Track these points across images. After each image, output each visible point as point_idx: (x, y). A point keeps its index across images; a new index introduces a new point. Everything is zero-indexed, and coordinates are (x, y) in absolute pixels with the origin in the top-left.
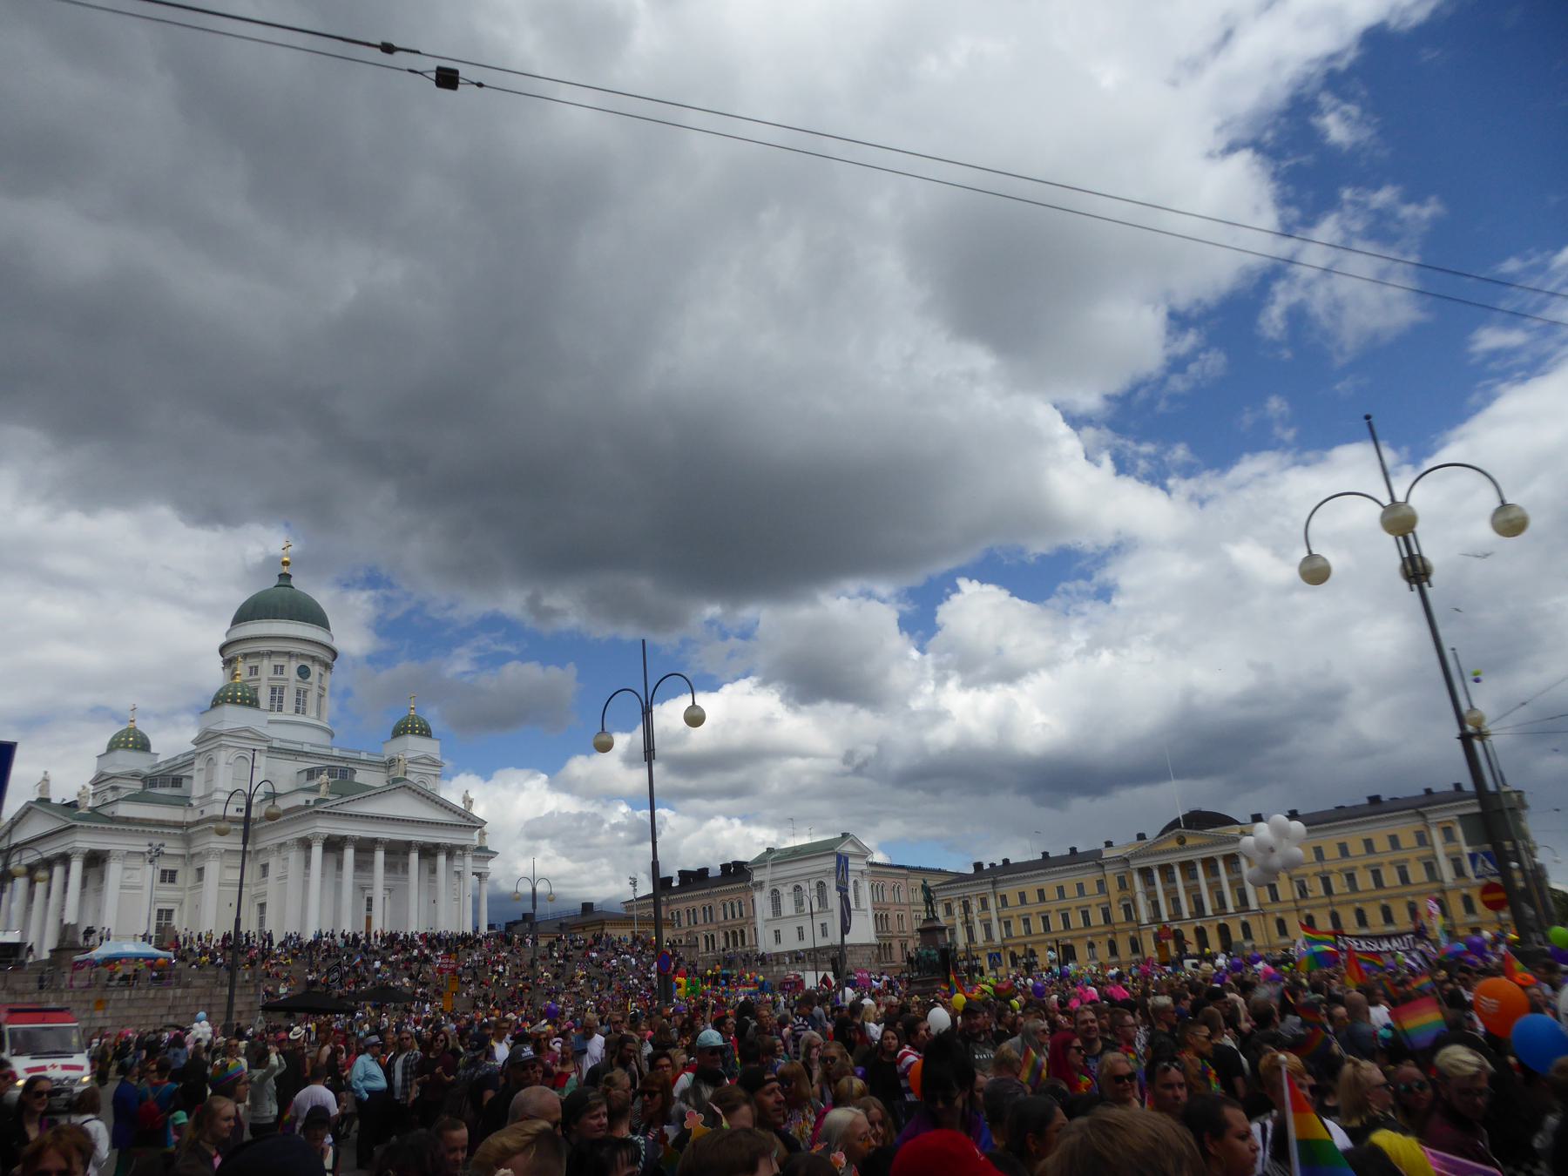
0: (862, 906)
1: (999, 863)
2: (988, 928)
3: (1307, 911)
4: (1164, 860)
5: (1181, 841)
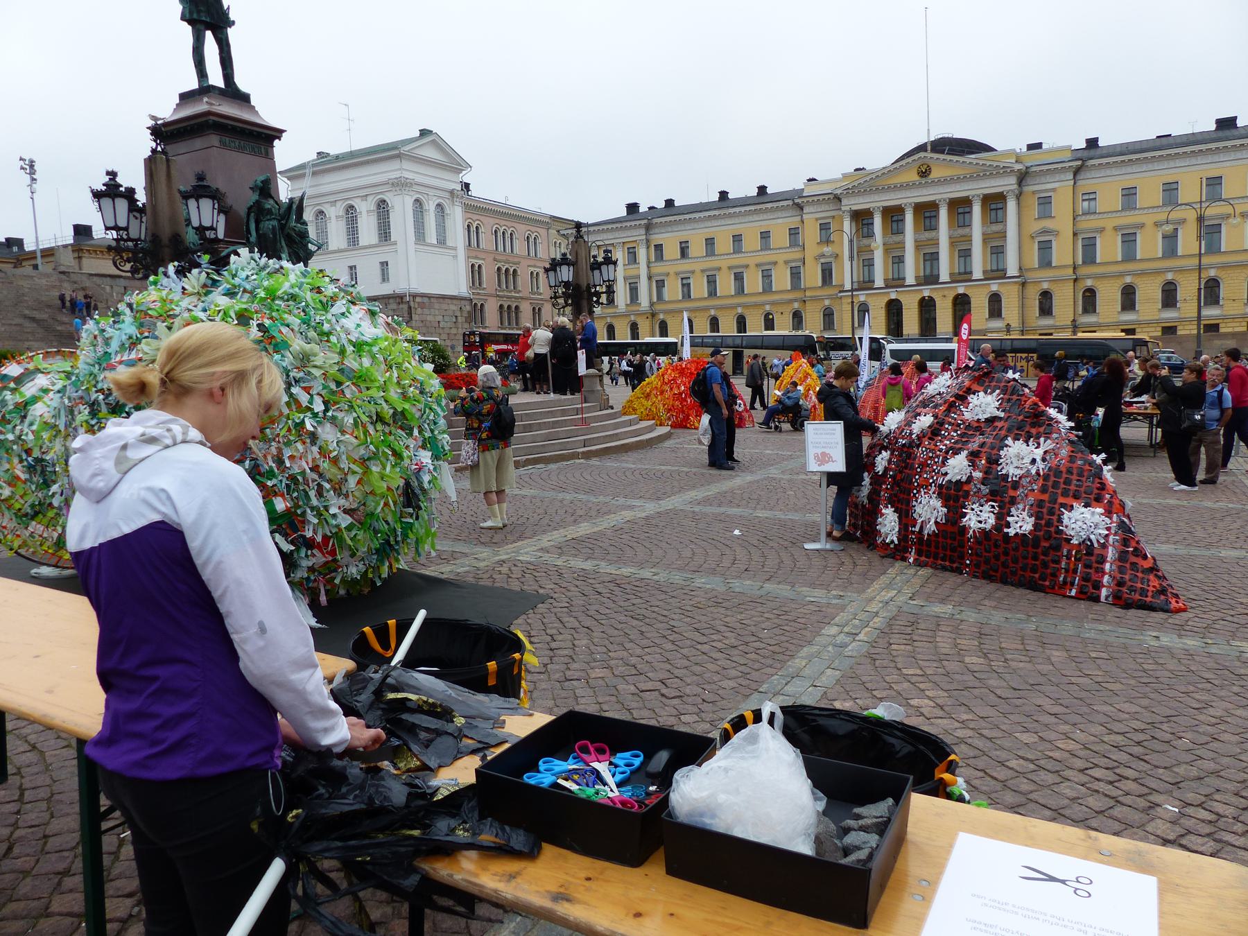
0: (450, 243)
1: (661, 204)
2: (634, 291)
3: (1089, 283)
4: (892, 200)
5: (924, 173)
